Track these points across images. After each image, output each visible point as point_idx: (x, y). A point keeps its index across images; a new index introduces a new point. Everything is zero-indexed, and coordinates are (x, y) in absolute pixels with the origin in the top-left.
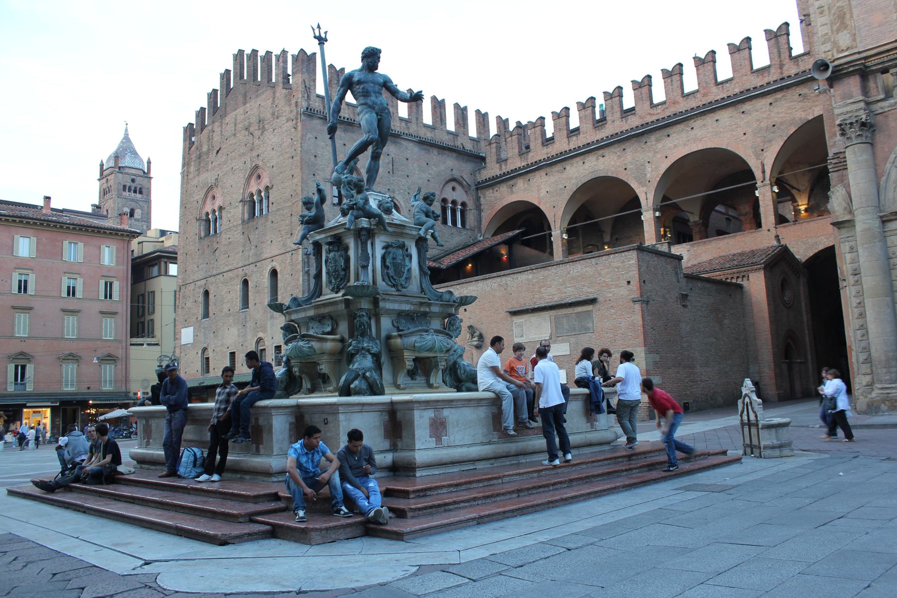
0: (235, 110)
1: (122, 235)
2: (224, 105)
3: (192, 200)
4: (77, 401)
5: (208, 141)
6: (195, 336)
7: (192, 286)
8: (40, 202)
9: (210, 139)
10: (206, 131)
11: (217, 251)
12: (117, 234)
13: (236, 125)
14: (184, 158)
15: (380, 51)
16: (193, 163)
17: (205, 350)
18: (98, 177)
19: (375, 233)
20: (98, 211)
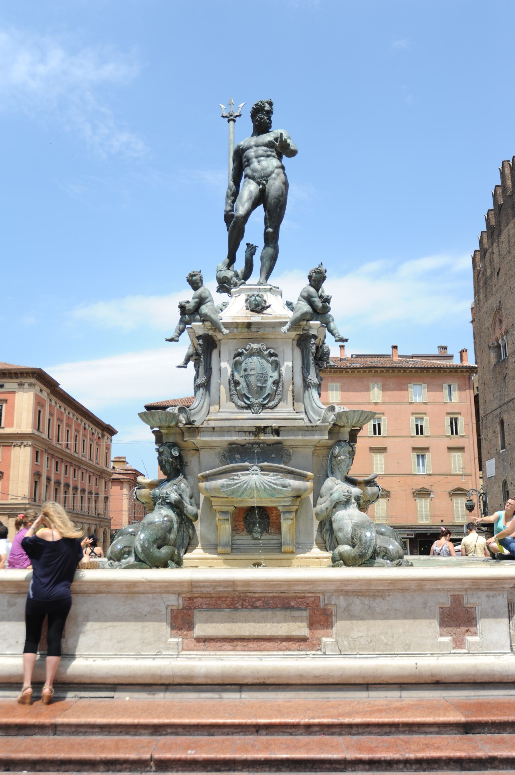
0: (507, 225)
1: (462, 372)
2: (499, 223)
3: (484, 327)
4: (431, 533)
5: (490, 264)
6: (497, 468)
7: (491, 415)
8: (389, 352)
9: (491, 261)
10: (488, 255)
11: (507, 377)
12: (456, 372)
13: (509, 241)
14: (475, 287)
15: (271, 104)
16: (481, 291)
17: (505, 483)
18: (471, 320)
19: (221, 340)
20: (445, 352)
